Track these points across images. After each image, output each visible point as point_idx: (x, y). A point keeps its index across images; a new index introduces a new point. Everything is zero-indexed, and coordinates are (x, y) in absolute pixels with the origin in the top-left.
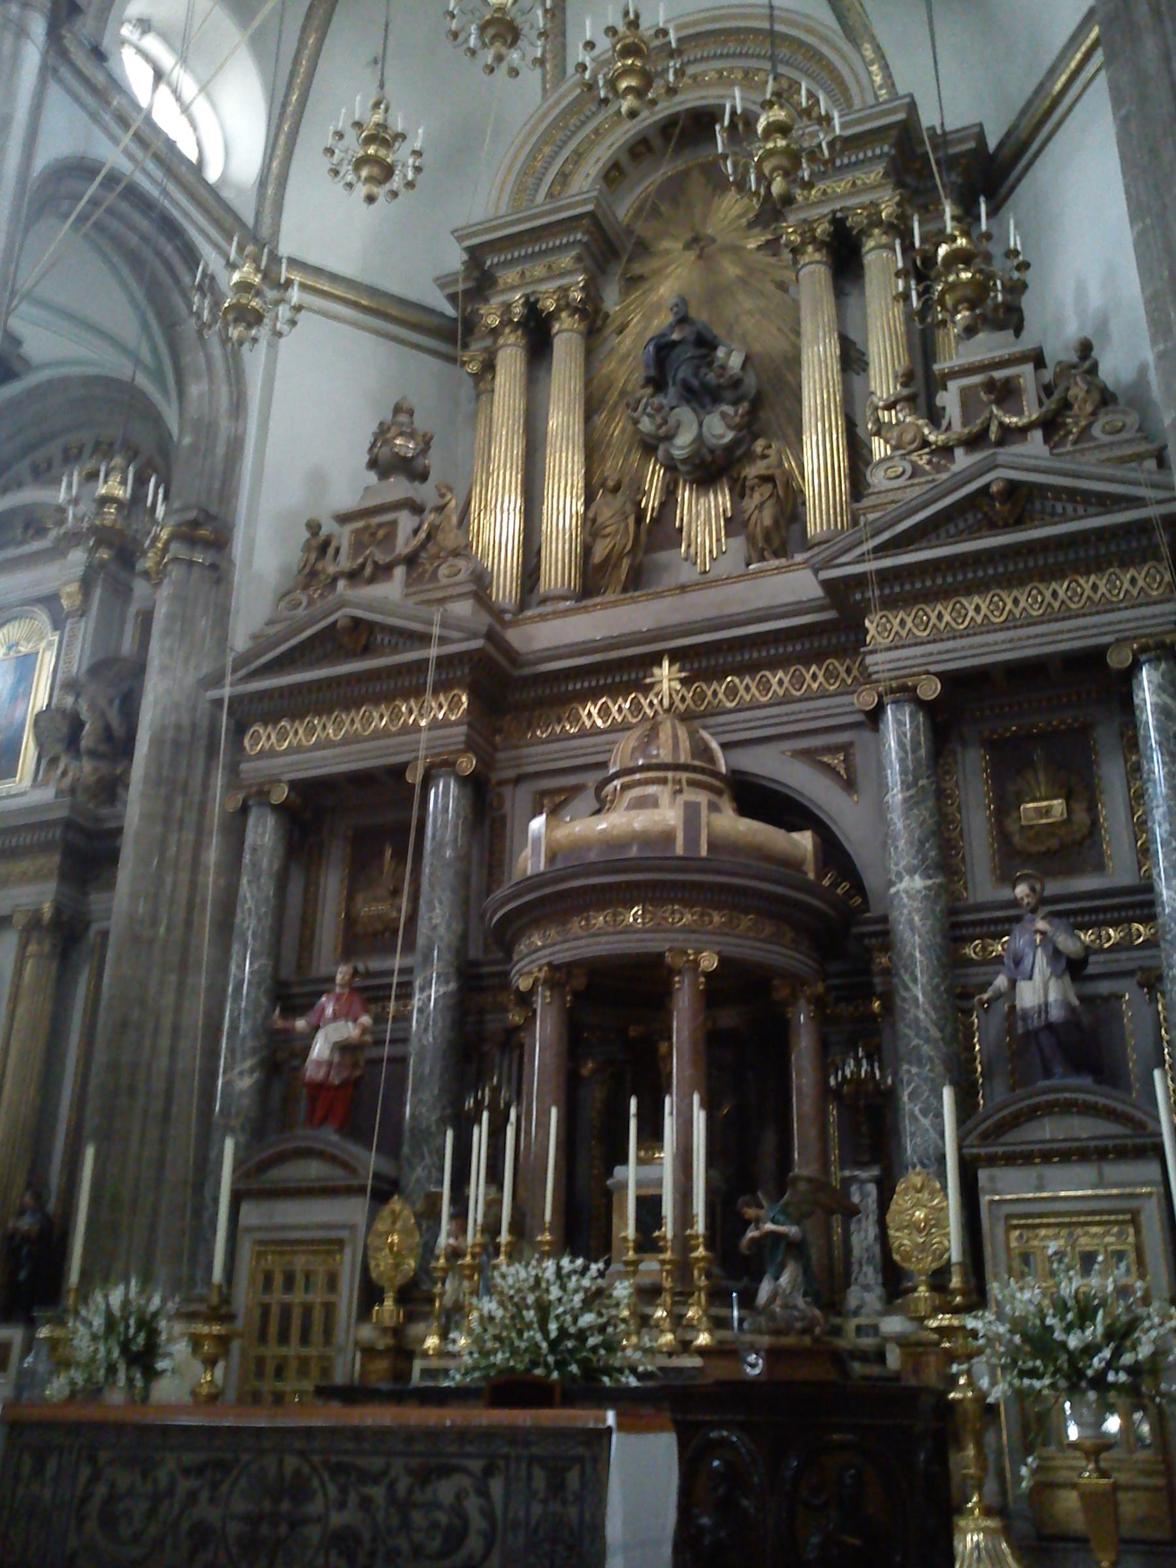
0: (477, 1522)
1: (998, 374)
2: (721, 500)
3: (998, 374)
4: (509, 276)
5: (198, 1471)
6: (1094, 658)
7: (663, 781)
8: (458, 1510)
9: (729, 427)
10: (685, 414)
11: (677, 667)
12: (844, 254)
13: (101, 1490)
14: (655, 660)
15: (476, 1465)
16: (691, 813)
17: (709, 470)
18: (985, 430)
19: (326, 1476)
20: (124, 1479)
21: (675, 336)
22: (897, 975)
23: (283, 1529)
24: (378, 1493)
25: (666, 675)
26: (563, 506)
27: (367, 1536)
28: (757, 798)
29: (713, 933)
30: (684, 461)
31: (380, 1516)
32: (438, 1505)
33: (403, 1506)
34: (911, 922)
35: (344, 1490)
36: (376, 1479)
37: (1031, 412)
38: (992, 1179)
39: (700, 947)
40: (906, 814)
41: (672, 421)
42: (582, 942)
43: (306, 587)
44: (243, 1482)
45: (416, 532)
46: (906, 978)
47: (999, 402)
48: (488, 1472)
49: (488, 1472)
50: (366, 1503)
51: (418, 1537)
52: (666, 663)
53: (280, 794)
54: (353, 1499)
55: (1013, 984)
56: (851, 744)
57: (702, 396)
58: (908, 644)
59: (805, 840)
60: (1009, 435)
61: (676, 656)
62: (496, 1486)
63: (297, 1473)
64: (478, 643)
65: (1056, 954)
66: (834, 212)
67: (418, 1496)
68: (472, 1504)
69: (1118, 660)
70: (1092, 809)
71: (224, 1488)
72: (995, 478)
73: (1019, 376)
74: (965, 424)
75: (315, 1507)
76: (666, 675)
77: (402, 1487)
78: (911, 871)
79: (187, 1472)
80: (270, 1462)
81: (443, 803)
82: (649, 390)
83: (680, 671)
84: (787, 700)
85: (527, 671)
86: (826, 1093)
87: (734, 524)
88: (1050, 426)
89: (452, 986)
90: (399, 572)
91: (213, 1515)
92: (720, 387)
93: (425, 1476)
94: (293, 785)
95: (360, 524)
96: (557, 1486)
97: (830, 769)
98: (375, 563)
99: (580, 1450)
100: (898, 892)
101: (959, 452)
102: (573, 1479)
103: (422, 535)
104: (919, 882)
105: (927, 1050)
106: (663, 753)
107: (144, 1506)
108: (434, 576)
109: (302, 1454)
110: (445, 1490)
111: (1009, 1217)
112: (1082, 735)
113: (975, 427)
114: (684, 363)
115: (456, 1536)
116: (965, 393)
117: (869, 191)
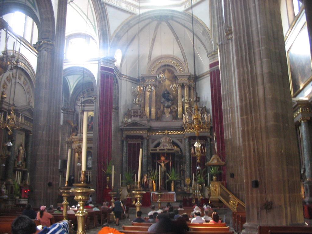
2: (169, 110)
10: (167, 102)
12: (183, 86)
17: (168, 107)
25: (166, 132)
26: (153, 110)
28: (174, 144)
40: (188, 148)
45: (140, 112)
57: (168, 100)
64: (149, 127)
90: (139, 116)
95: (134, 110)
97: (180, 141)
103: (141, 112)
106: (167, 141)
108: (143, 118)
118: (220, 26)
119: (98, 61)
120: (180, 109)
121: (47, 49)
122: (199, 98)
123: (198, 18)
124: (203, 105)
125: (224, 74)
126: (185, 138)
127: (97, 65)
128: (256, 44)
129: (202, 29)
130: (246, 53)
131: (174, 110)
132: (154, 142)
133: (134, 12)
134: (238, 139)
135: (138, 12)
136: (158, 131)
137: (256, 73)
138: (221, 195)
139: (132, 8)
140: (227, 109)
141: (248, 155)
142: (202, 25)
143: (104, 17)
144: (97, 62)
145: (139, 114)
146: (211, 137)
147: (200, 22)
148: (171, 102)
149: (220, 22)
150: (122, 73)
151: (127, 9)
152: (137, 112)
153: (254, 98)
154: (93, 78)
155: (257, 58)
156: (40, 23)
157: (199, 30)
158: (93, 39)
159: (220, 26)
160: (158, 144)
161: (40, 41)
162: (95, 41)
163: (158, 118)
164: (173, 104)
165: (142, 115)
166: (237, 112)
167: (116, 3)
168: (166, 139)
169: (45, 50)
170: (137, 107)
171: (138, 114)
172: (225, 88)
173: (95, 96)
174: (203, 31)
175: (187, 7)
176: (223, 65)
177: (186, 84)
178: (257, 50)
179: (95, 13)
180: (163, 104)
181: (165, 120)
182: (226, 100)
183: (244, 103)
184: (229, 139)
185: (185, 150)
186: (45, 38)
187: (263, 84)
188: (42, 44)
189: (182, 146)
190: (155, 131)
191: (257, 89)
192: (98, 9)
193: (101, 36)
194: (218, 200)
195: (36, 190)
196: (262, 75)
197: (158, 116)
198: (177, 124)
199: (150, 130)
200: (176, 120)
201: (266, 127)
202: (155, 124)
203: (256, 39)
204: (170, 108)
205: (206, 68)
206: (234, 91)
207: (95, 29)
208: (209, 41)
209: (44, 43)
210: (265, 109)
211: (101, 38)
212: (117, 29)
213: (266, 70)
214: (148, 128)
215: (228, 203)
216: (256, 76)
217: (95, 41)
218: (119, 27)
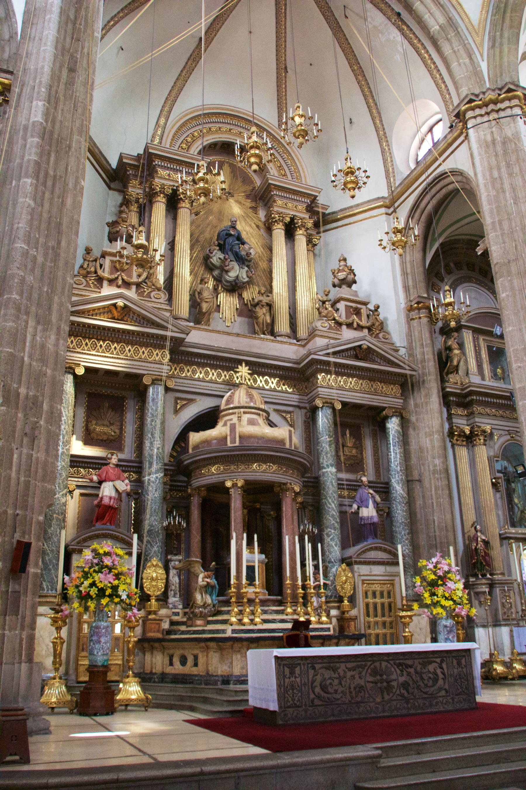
0: (441, 676)
1: (359, 306)
3: (359, 306)
4: (162, 172)
5: (353, 669)
6: (379, 410)
7: (259, 415)
8: (435, 673)
9: (248, 277)
11: (247, 368)
13: (319, 678)
14: (240, 362)
15: (438, 660)
17: (234, 288)
18: (353, 323)
19: (395, 667)
20: (328, 674)
21: (232, 233)
22: (326, 498)
23: (385, 684)
24: (412, 670)
25: (244, 370)
27: (411, 683)
29: (271, 473)
30: (227, 281)
31: (414, 677)
32: (429, 672)
34: (332, 482)
35: (402, 671)
36: (411, 667)
38: (358, 568)
40: (330, 445)
41: (230, 266)
42: (258, 474)
43: (85, 277)
44: (369, 671)
46: (330, 501)
47: (356, 315)
48: (442, 661)
49: (442, 661)
50: (409, 674)
51: (426, 682)
52: (244, 365)
53: (80, 371)
54: (405, 673)
55: (358, 509)
56: (293, 412)
60: (360, 328)
61: (248, 363)
62: (444, 666)
63: (386, 666)
65: (375, 502)
66: (294, 216)
67: (424, 671)
68: (439, 671)
70: (362, 453)
71: (363, 674)
72: (365, 344)
73: (361, 309)
74: (347, 317)
75: (394, 677)
76: (244, 370)
77: (419, 669)
78: (332, 465)
79: (350, 670)
80: (377, 664)
82: (218, 248)
83: (249, 370)
84: (274, 390)
85: (183, 349)
87: (240, 313)
88: (369, 329)
89: (162, 475)
90: (134, 288)
91: (362, 682)
92: (247, 260)
93: (424, 665)
94: (87, 369)
96: (459, 664)
97: (285, 419)
98: (123, 280)
99: (464, 654)
100: (327, 472)
101: (344, 327)
102: (463, 661)
105: (336, 525)
107: (336, 682)
108: (149, 296)
109: (387, 661)
110: (431, 668)
111: (363, 580)
113: (350, 321)
114: (229, 241)
132: (183, 407)
148: (246, 268)
160: (208, 419)
164: (250, 282)
171: (131, 276)
180: (216, 273)
200: (272, 338)
204: (240, 296)
208: (467, 61)
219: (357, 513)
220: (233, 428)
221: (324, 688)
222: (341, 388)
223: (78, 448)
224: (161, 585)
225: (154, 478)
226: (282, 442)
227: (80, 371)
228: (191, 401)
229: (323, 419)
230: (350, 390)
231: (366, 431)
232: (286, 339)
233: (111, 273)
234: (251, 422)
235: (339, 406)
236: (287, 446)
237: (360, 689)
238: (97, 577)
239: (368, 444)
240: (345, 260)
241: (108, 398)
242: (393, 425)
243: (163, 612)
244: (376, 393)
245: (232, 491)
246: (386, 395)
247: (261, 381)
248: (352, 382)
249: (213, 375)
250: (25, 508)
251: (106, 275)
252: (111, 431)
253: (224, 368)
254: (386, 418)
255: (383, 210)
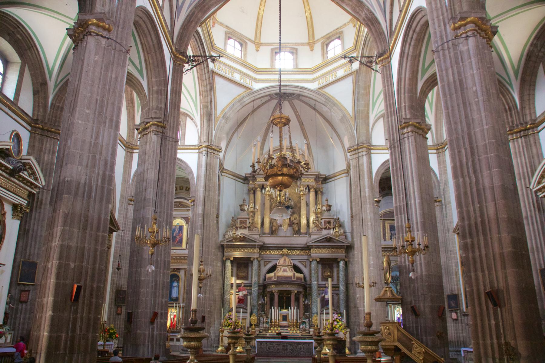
16: (294, 274)
25: (285, 251)
33: (296, 347)
37: (332, 226)
39: (295, 290)
43: (232, 227)
58: (317, 254)
59: (302, 276)
60: (329, 229)
69: (339, 260)
81: (255, 263)
84: (298, 255)
86: (304, 305)
104: (316, 283)
106: (287, 263)
110: (300, 346)
112: (332, 264)
115: (301, 349)
116: (325, 221)
117: (311, 181)
118: (391, 116)
119: (199, 149)
120: (304, 221)
121: (156, 133)
122: (330, 206)
123: (337, 100)
124: (334, 215)
125: (397, 179)
126: (311, 260)
127: (197, 155)
128: (481, 150)
129: (341, 115)
130: (467, 159)
131: (295, 221)
133: (250, 86)
134: (419, 265)
135: (257, 86)
136: (272, 250)
137: (483, 186)
138: (398, 341)
139: (248, 80)
140: (402, 226)
141: (475, 289)
142: (341, 109)
143: (211, 90)
144: (197, 151)
145: (248, 225)
146: (347, 260)
147: (339, 105)
148: (290, 210)
149: (391, 112)
150: (225, 168)
151: (242, 82)
152: (245, 222)
153: (482, 215)
154: (191, 172)
155: (484, 167)
156: (145, 95)
157: (336, 117)
158: (192, 119)
159: (391, 116)
160: (273, 269)
161: (149, 121)
162: (195, 123)
163: (273, 232)
165: (251, 227)
166: (418, 231)
167: (227, 73)
168: (285, 260)
169: (155, 134)
170: (244, 215)
171: (246, 225)
172: (400, 198)
173: (193, 199)
174: (342, 118)
175: (322, 85)
176: (396, 166)
177: (313, 187)
178: (483, 157)
179: (199, 84)
181: (282, 234)
182: (401, 214)
183: (466, 222)
184: (405, 265)
185: (311, 276)
186: (155, 118)
187: (494, 200)
188: (151, 126)
189: (305, 270)
190: (269, 249)
191: (486, 206)
192: (204, 79)
193: (205, 116)
194: (393, 347)
195: (138, 332)
196: (492, 188)
197: (274, 228)
198: (301, 240)
199: (263, 247)
200: (297, 236)
201: (502, 255)
202: (269, 240)
203: (481, 143)
205: (341, 166)
206: (413, 202)
207: (196, 106)
209: (154, 124)
210: (499, 232)
211: (205, 118)
212: (226, 107)
213: (497, 183)
214: (260, 245)
215: (411, 351)
216: (484, 189)
217: (195, 123)
218: (228, 105)
219: (324, 296)
220: (275, 274)
221: (269, 349)
222: (320, 253)
223: (233, 280)
224: (256, 321)
225: (255, 289)
226: (291, 277)
227: (232, 259)
228: (270, 262)
229: (314, 264)
230: (324, 253)
231: (335, 265)
232: (304, 235)
233: (240, 224)
234: (285, 271)
235: (318, 260)
236: (293, 279)
237: (278, 349)
238: (229, 321)
239: (335, 270)
240: (327, 200)
241: (242, 265)
242: (342, 264)
243: (257, 329)
244: (334, 253)
245: (275, 294)
246: (339, 253)
247: (294, 252)
248: (324, 250)
249: (276, 252)
250: (204, 308)
251: (238, 225)
252: (244, 274)
253: (280, 250)
254: (339, 262)
255: (345, 175)
